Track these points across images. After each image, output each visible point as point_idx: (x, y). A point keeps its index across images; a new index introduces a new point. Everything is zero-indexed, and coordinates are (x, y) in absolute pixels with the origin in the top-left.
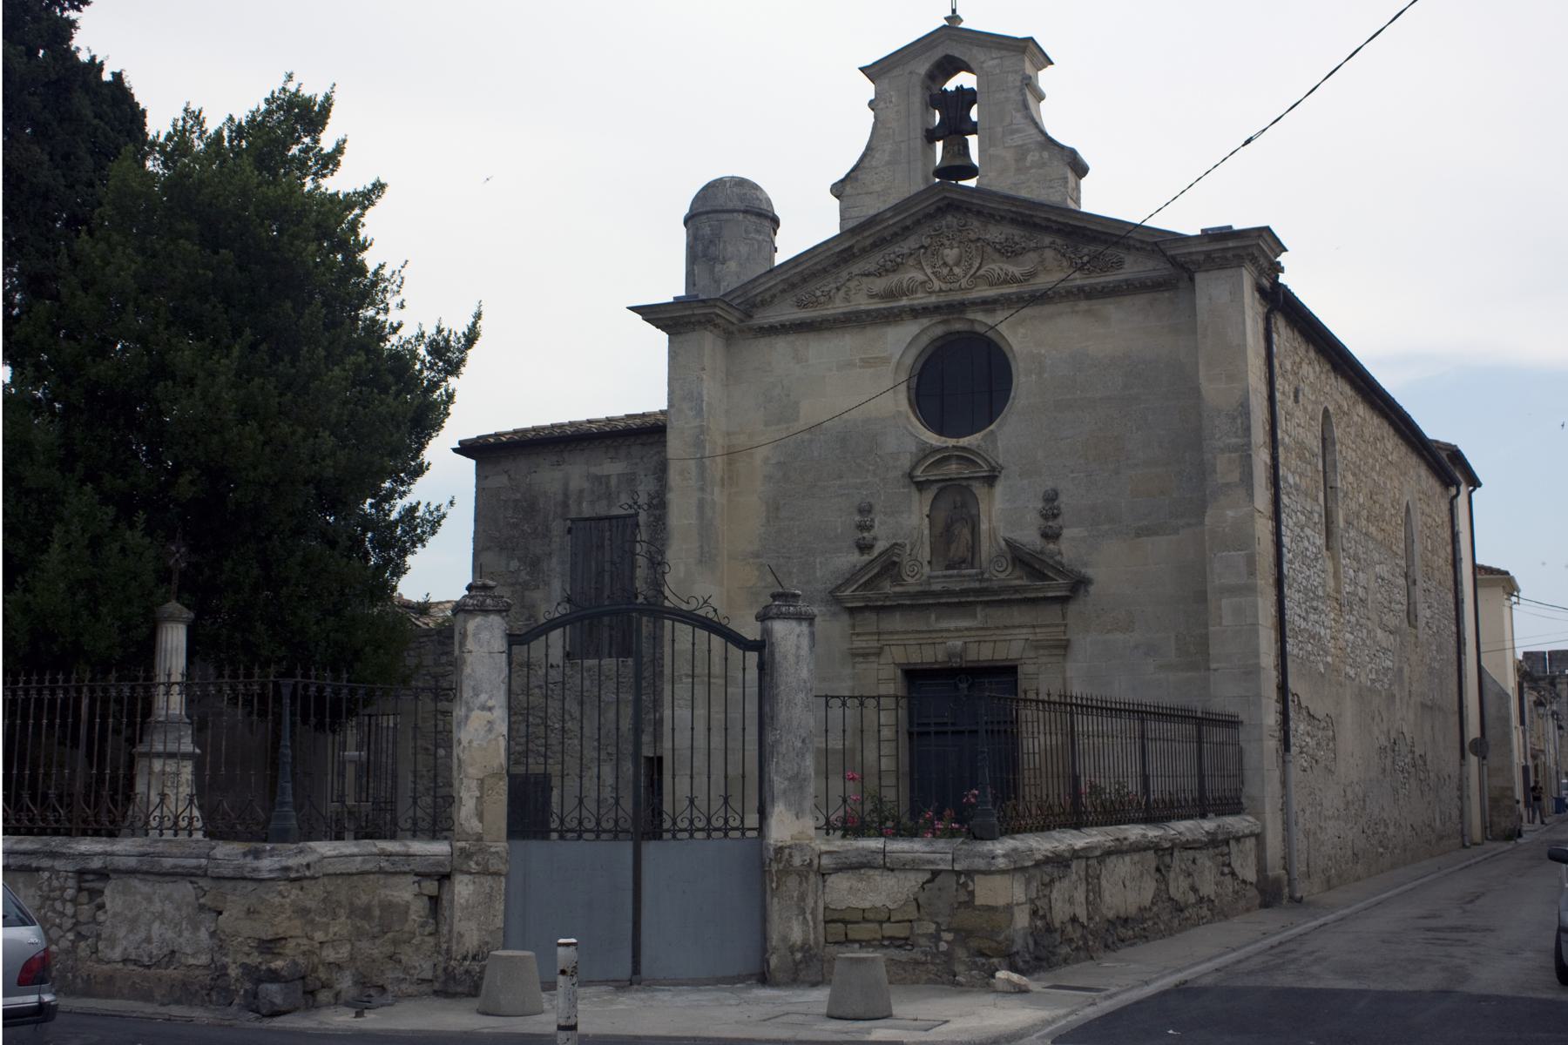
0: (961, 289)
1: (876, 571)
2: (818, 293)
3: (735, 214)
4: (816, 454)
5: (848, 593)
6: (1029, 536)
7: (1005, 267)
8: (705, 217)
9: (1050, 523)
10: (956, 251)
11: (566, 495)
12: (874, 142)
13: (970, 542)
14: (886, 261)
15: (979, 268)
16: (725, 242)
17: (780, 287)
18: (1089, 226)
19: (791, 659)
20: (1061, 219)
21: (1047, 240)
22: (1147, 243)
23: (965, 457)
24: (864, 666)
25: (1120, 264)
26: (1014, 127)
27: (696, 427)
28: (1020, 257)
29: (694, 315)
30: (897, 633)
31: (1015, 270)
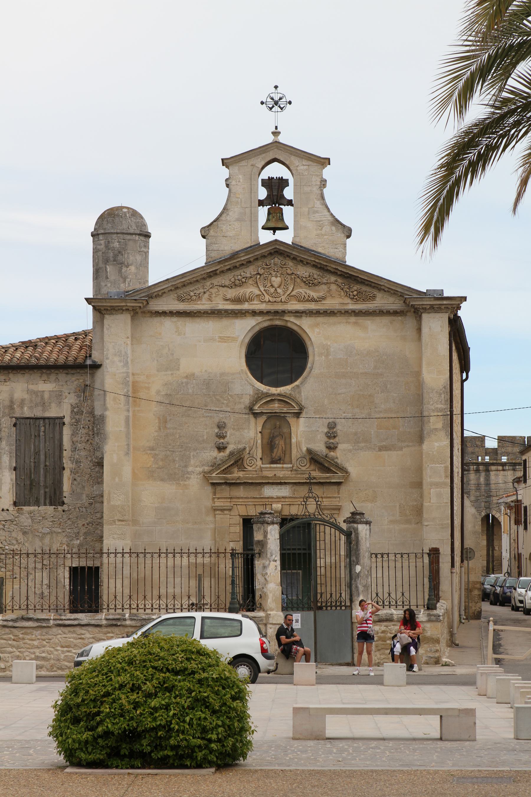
0: (281, 301)
1: (232, 463)
2: (192, 294)
3: (134, 236)
4: (190, 391)
5: (214, 475)
6: (320, 447)
7: (308, 291)
8: (115, 235)
9: (332, 441)
10: (279, 279)
11: (12, 402)
12: (228, 205)
13: (284, 448)
14: (235, 280)
15: (292, 291)
16: (128, 253)
17: (169, 289)
18: (360, 276)
19: (364, 539)
20: (345, 270)
21: (333, 279)
22: (392, 289)
23: (283, 400)
24: (222, 516)
25: (374, 297)
26: (316, 209)
27: (123, 373)
28: (317, 287)
29: (127, 306)
30: (242, 498)
31: (314, 294)
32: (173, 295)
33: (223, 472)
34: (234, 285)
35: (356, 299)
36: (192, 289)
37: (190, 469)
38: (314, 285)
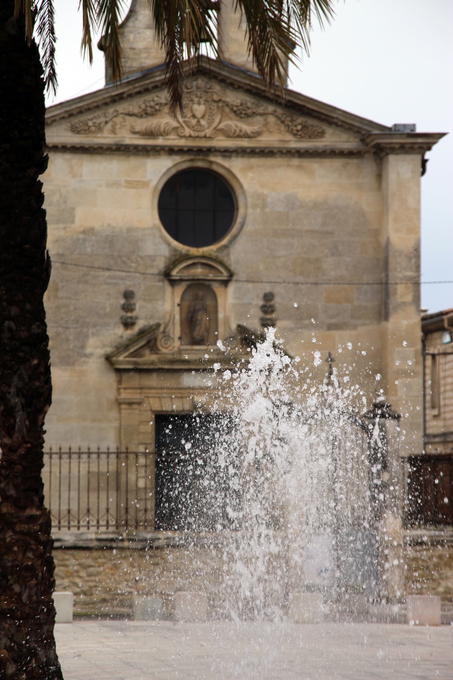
2: (90, 123)
4: (89, 250)
14: (146, 106)
15: (220, 123)
17: (62, 116)
21: (271, 108)
24: (128, 411)
25: (322, 134)
30: (155, 388)
31: (247, 128)
32: (65, 125)
33: (132, 355)
34: (145, 114)
35: (300, 135)
36: (90, 116)
37: (88, 350)
38: (248, 116)
